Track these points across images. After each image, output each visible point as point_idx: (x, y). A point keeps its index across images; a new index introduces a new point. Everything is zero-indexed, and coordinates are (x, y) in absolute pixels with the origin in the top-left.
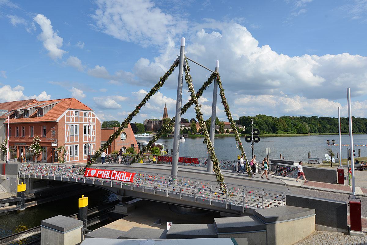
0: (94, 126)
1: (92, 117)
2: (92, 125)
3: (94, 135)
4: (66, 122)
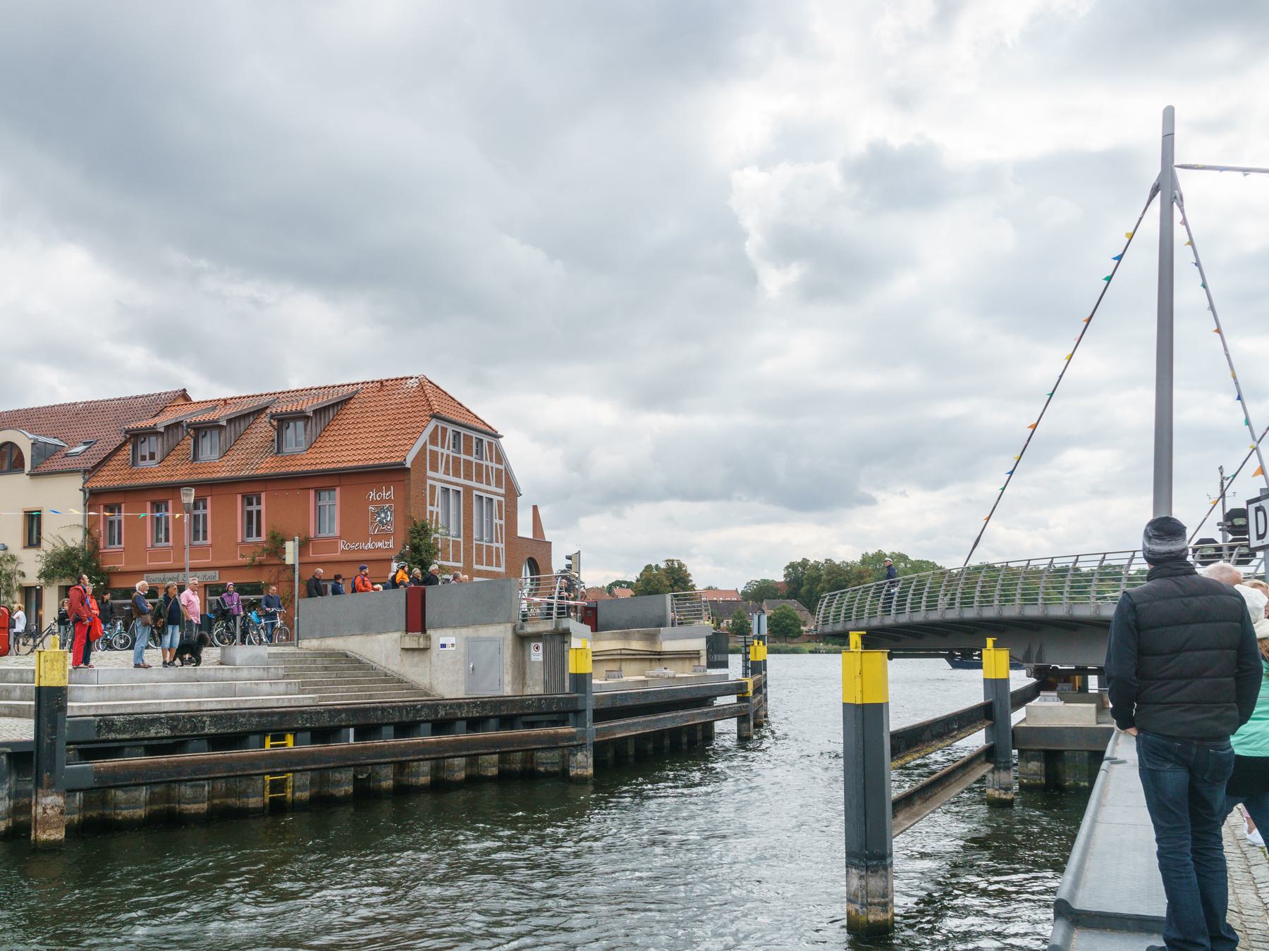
0: (500, 503)
2: (496, 498)
4: (429, 473)
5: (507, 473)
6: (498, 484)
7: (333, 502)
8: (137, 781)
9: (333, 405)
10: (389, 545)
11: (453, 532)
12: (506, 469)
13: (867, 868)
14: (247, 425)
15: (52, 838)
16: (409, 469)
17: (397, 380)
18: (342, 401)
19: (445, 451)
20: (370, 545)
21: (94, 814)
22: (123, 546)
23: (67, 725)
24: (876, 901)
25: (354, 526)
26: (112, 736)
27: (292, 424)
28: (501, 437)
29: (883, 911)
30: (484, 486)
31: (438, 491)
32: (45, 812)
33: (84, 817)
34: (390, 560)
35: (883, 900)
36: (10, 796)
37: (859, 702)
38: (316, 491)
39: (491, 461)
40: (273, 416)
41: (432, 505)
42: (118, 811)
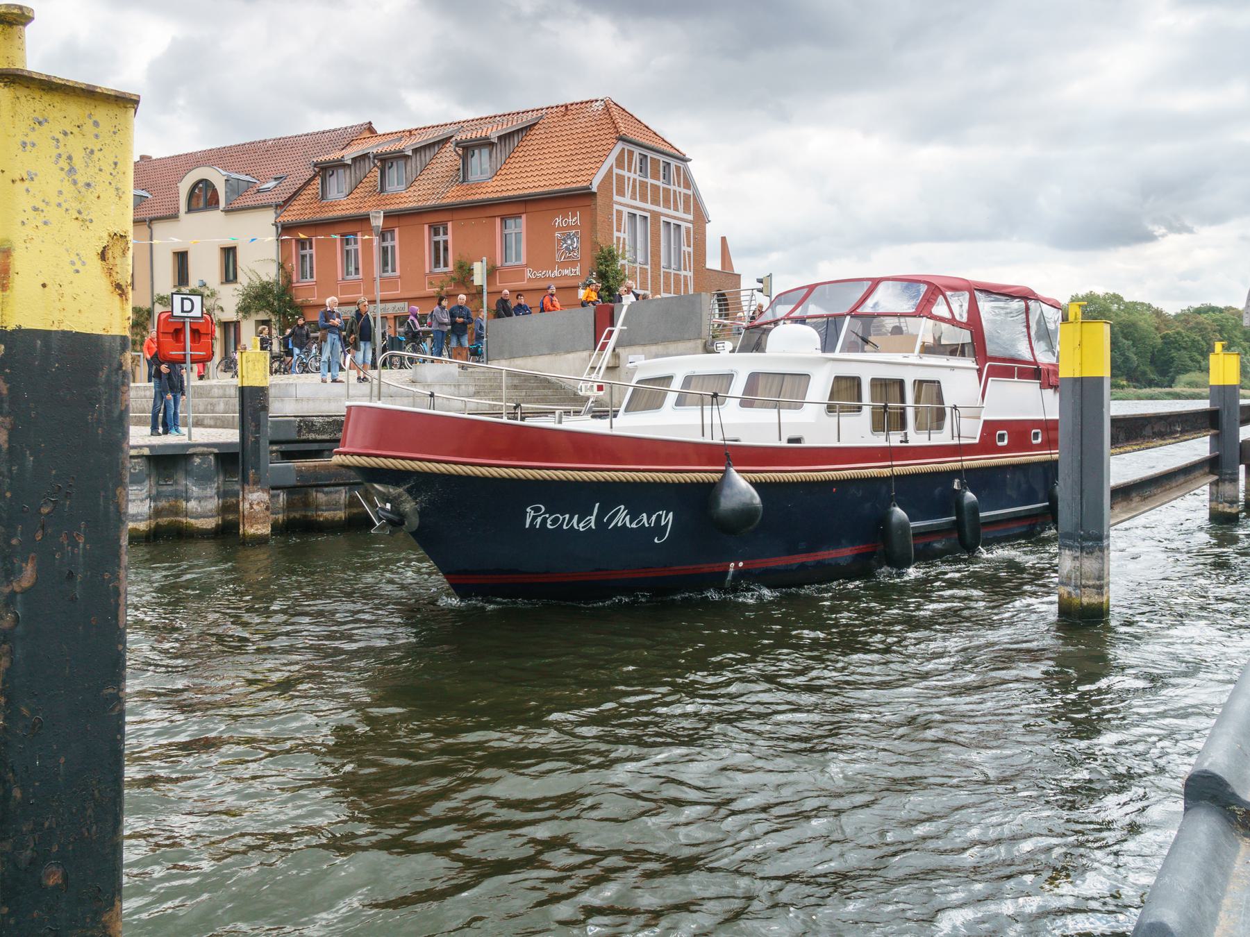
0: (688, 230)
2: (683, 225)
4: (616, 198)
5: (695, 199)
6: (687, 210)
7: (519, 228)
8: (337, 481)
9: (518, 131)
11: (640, 259)
13: (1082, 549)
14: (432, 154)
15: (259, 532)
16: (594, 194)
17: (582, 103)
18: (526, 128)
19: (632, 175)
21: (297, 515)
22: (315, 279)
23: (269, 424)
24: (1091, 583)
25: (540, 254)
26: (312, 436)
27: (476, 152)
29: (1098, 594)
30: (671, 212)
31: (625, 217)
32: (252, 508)
33: (288, 517)
34: (578, 287)
35: (1098, 583)
36: (218, 494)
37: (1077, 375)
38: (502, 219)
39: (679, 186)
40: (457, 144)
41: (619, 230)
42: (320, 513)
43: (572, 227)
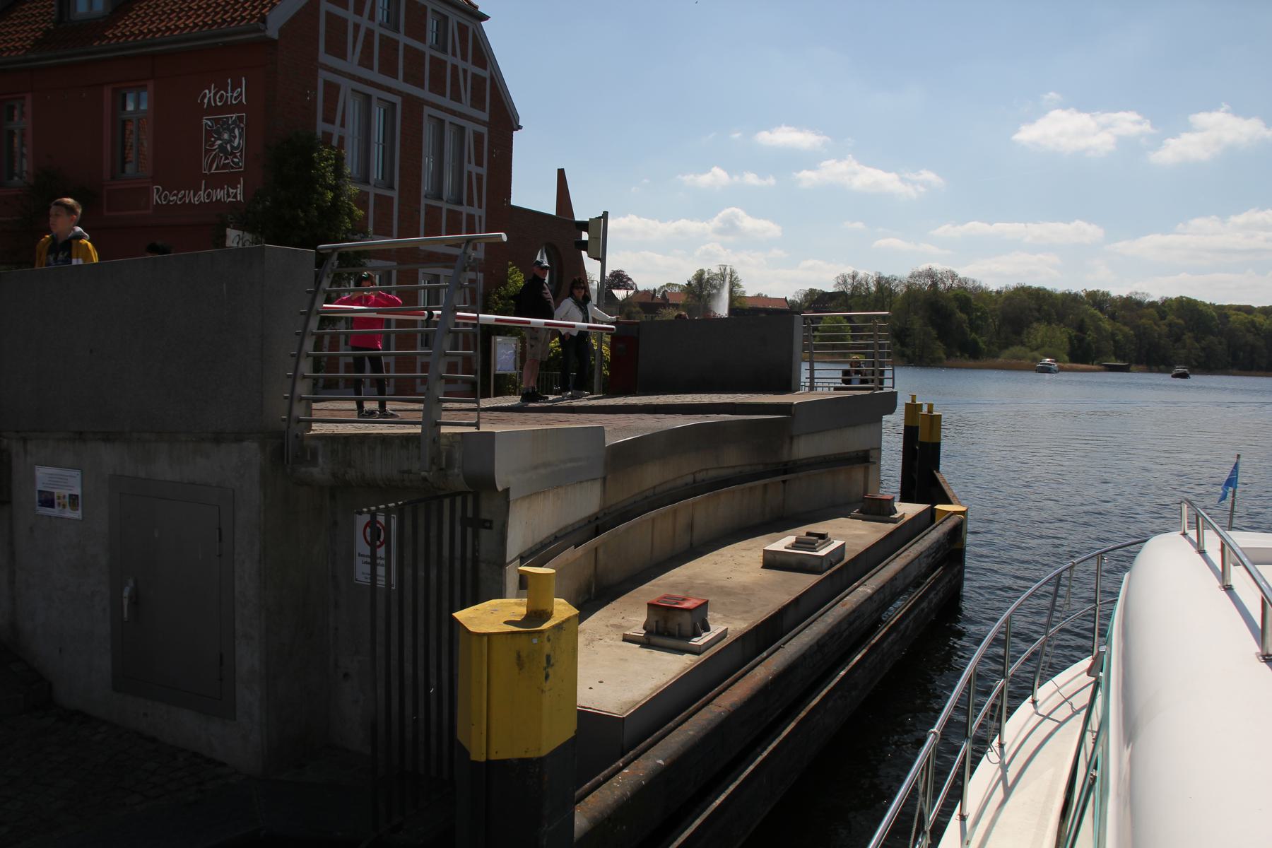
0: (478, 137)
1: (473, 69)
2: (470, 127)
3: (480, 207)
4: (324, 58)
5: (492, 79)
6: (477, 101)
10: (235, 196)
11: (376, 173)
12: (492, 79)
20: (202, 196)
28: (485, 18)
30: (446, 102)
41: (329, 119)
43: (227, 108)
